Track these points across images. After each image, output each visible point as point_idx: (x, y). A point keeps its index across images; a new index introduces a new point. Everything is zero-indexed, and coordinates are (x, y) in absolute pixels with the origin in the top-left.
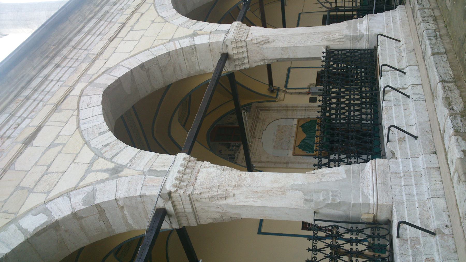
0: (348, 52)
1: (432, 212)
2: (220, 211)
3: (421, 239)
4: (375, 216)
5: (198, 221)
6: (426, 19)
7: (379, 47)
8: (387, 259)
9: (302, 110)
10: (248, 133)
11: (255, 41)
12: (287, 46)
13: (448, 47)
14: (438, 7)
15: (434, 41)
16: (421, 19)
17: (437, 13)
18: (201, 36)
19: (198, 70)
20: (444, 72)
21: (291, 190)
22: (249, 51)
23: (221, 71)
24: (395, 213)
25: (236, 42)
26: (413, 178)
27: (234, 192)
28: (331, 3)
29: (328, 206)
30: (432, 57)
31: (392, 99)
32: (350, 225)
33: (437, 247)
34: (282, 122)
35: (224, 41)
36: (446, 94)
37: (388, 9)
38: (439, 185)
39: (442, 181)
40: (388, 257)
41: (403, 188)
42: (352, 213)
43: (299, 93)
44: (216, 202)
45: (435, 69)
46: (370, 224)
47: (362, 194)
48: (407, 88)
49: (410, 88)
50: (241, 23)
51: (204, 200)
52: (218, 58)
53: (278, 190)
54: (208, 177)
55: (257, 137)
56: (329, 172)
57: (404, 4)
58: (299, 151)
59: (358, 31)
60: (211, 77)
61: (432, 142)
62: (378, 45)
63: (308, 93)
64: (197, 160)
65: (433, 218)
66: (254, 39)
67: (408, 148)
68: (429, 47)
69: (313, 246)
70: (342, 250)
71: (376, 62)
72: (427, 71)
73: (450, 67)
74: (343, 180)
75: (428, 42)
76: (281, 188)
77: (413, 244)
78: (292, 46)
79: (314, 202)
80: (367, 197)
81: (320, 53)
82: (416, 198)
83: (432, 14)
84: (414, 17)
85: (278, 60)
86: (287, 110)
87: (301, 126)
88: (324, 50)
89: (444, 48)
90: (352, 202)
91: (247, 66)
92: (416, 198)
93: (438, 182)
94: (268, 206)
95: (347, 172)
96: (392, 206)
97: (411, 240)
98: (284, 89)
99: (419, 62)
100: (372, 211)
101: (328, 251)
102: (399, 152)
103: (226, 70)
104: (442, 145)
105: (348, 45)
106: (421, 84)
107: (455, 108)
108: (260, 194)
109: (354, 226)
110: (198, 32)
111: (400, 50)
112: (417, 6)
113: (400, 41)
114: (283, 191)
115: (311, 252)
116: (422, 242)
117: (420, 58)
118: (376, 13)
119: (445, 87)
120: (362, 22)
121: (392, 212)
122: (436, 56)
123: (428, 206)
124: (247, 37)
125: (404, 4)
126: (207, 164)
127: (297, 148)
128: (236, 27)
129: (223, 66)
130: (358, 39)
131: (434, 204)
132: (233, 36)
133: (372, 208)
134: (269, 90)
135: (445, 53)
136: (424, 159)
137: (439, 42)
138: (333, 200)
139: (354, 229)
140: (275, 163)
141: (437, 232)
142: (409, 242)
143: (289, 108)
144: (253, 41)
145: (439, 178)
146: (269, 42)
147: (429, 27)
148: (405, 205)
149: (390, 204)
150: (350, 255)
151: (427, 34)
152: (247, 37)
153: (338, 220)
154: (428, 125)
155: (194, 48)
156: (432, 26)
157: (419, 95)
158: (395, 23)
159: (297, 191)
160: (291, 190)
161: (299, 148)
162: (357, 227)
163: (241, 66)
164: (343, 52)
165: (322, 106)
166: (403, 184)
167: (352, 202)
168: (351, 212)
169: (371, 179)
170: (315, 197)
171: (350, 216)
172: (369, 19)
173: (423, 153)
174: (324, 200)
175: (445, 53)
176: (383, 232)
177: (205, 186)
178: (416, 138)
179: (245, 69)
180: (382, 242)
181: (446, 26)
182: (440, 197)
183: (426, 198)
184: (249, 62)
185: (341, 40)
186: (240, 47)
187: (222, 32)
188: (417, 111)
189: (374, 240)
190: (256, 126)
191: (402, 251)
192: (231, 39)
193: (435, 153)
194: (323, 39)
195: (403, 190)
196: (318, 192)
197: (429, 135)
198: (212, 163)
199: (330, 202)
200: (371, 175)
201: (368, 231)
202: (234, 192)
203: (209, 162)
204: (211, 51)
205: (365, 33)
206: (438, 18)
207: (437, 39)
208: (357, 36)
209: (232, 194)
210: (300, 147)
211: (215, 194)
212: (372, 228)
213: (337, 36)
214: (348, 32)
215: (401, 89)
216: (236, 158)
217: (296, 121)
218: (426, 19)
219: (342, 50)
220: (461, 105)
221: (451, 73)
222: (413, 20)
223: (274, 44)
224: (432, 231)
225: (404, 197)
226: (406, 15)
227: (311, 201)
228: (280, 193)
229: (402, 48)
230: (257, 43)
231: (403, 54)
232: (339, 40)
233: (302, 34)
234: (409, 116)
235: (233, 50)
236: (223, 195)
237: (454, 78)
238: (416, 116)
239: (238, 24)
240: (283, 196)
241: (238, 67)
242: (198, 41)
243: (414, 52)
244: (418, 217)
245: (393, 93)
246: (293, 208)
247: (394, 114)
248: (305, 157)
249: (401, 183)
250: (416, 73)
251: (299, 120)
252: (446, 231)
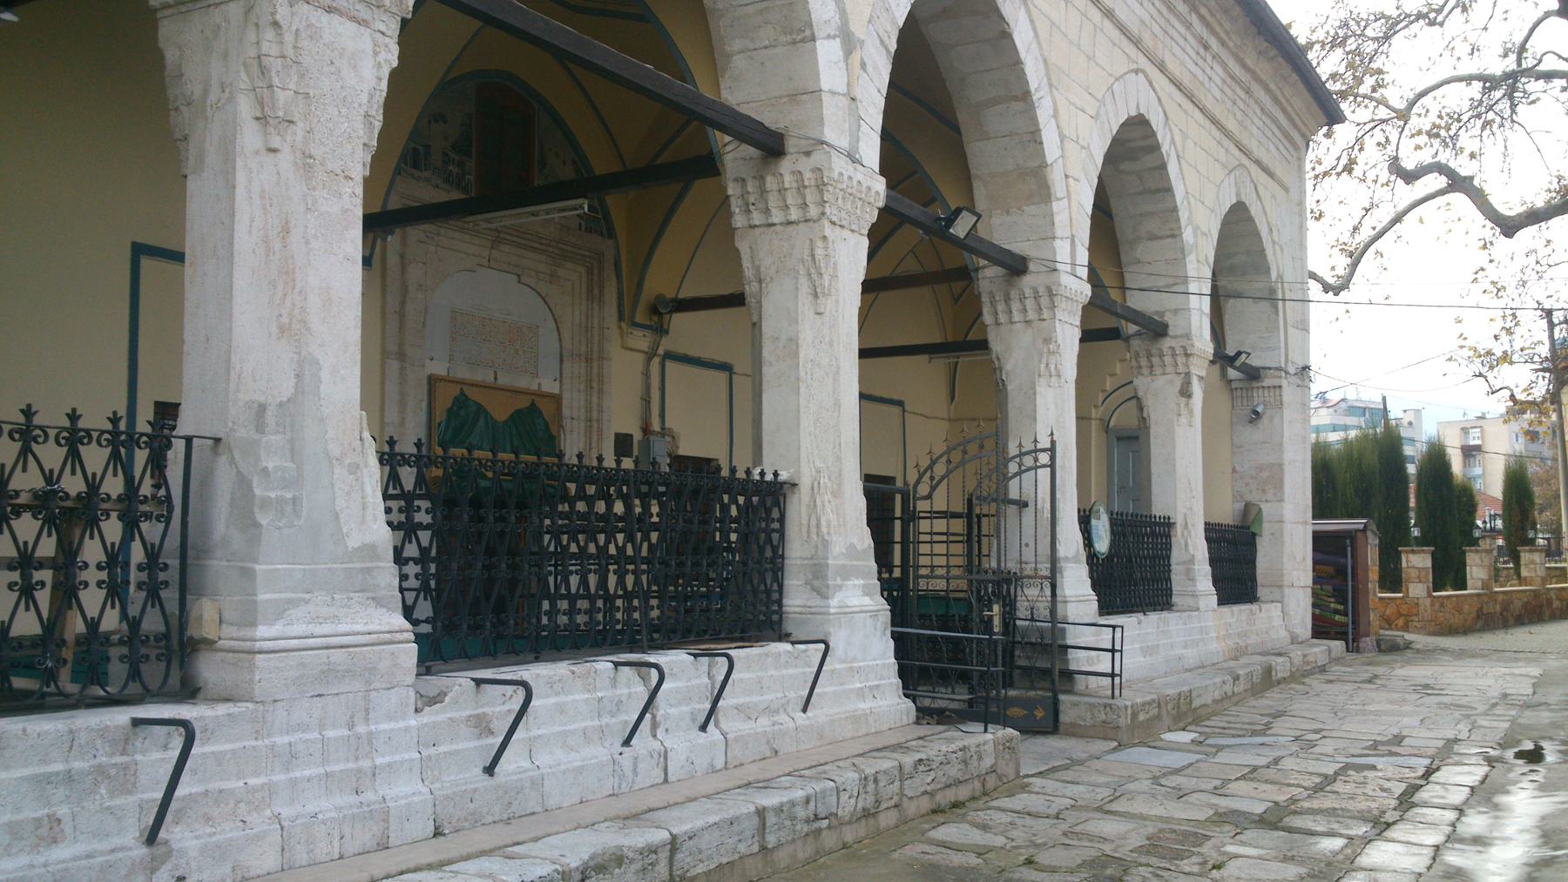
0: (775, 549)
1: (229, 831)
2: (212, 98)
3: (130, 799)
4: (209, 643)
5: (170, 11)
6: (871, 787)
7: (788, 647)
8: (52, 688)
9: (589, 409)
10: (506, 219)
11: (819, 252)
12: (802, 355)
13: (782, 857)
14: (904, 821)
15: (801, 813)
16: (869, 771)
17: (887, 819)
18: (842, 65)
19: (728, 49)
20: (704, 847)
21: (296, 357)
22: (790, 228)
23: (724, 129)
24: (222, 709)
25: (821, 186)
26: (351, 765)
27: (286, 149)
28: (929, 497)
29: (244, 483)
30: (753, 809)
31: (618, 692)
32: (174, 563)
33: (102, 853)
34: (548, 342)
35: (823, 143)
36: (631, 855)
37: (903, 673)
38: (325, 848)
39: (341, 858)
40: (60, 693)
42: (218, 565)
43: (646, 401)
44: (244, 82)
45: (716, 818)
46: (183, 627)
47: (289, 601)
48: (654, 736)
49: (656, 745)
50: (881, 204)
51: (251, 36)
52: (770, 119)
53: (297, 311)
54: (341, 55)
55: (495, 253)
56: (369, 490)
57: (918, 722)
59: (839, 581)
60: (706, 91)
61: (476, 821)
62: (793, 643)
63: (646, 430)
64: (404, 22)
65: (210, 835)
66: (826, 248)
67: (454, 747)
68: (785, 799)
69: (88, 432)
70: (78, 532)
71: (742, 639)
72: (708, 797)
73: (720, 866)
75: (799, 794)
76: (303, 322)
77: (113, 772)
78: (802, 373)
79: (257, 436)
80: (278, 616)
81: (774, 464)
82: (279, 777)
83: (884, 806)
84: (878, 750)
85: (756, 326)
86: (589, 360)
87: (533, 404)
88: (784, 476)
89: (780, 845)
90: (258, 567)
91: (739, 221)
92: (279, 777)
93: (336, 844)
94: (237, 274)
95: (369, 550)
96: (250, 700)
97: (125, 767)
98: (661, 351)
99: (738, 772)
100: (229, 635)
101: (73, 485)
102: (441, 717)
103: (729, 148)
104: (465, 851)
105: (796, 551)
106: (666, 781)
108: (278, 246)
109: (172, 575)
110: (856, 57)
111: (777, 711)
112: (908, 760)
113: (804, 710)
114: (292, 330)
115: (67, 423)
116: (118, 802)
117: (752, 772)
118: (894, 636)
119: (655, 852)
120: (867, 592)
121: (227, 700)
122: (756, 820)
123: (253, 818)
124: (833, 223)
125: (918, 722)
126: (391, 56)
127: (455, 391)
128: (869, 188)
129: (741, 138)
130: (816, 583)
131: (260, 837)
132: (841, 174)
133: (241, 634)
134: (660, 298)
135: (763, 848)
136: (416, 799)
137: (798, 827)
138: (266, 504)
139: (162, 576)
140: (401, 314)
141: (158, 850)
142: (119, 759)
143: (595, 364)
144: (820, 243)
145: (350, 849)
146: (816, 296)
147: (844, 797)
148: (254, 743)
149: (257, 692)
150: (61, 560)
151: (824, 791)
152: (833, 223)
153: (190, 519)
154: (533, 805)
155: (801, 35)
156: (847, 806)
158: (860, 694)
159: (293, 381)
160: (296, 357)
161: (456, 399)
162: (166, 583)
163: (740, 202)
164: (775, 536)
165: (599, 468)
166: (330, 733)
167: (258, 567)
168: (225, 563)
169: (342, 628)
170: (274, 439)
171: (209, 562)
172: (874, 614)
173: (437, 793)
174: (265, 470)
175: (763, 848)
176: (153, 672)
177: (304, 43)
178: (490, 770)
179: (730, 215)
180: (117, 670)
181: (845, 846)
182: (286, 855)
183: (277, 810)
184: (752, 227)
185: (814, 530)
186: (804, 197)
187: (855, 139)
188: (580, 770)
189: (121, 642)
190: (534, 249)
191: (83, 738)
192: (830, 169)
193: (438, 833)
194: (818, 471)
195: (307, 736)
196: (292, 450)
198: (394, 76)
199: (257, 491)
200: (359, 628)
201: (152, 623)
202: (286, 149)
203: (395, 64)
204: (793, 97)
205: (834, 602)
206: (872, 821)
207: (808, 821)
208: (825, 577)
209: (276, 142)
210: (461, 401)
211: (276, 81)
212: (166, 636)
213: (829, 516)
214: (838, 547)
215: (654, 717)
217: (550, 386)
218: (871, 787)
219: (782, 532)
221: (700, 869)
222: (867, 748)
223: (810, 314)
224: (162, 834)
225: (282, 740)
226: (886, 727)
227: (260, 428)
228: (285, 320)
229: (782, 718)
230: (813, 256)
231: (764, 723)
232: (813, 522)
233: (837, 404)
235: (793, 173)
236: (273, 108)
237: (682, 878)
238: (563, 767)
239: (877, 193)
240: (274, 330)
241: (739, 191)
242: (828, 52)
243: (768, 754)
244: (210, 786)
245: (641, 692)
246: (228, 361)
247: (570, 698)
248: (423, 417)
249: (334, 726)
250: (702, 764)
251: (556, 399)
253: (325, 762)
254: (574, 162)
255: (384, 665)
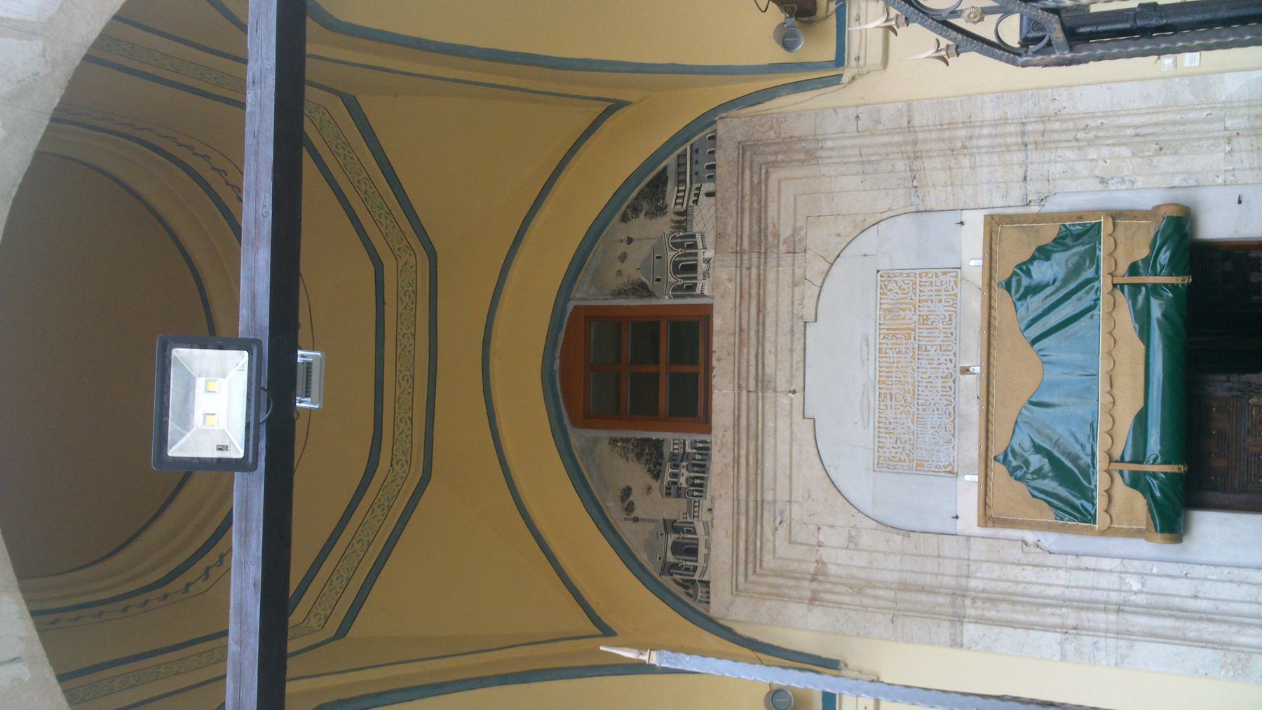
55: (782, 384)
58: (1009, 491)
190: (761, 308)
216: (702, 550)
254: (625, 219)
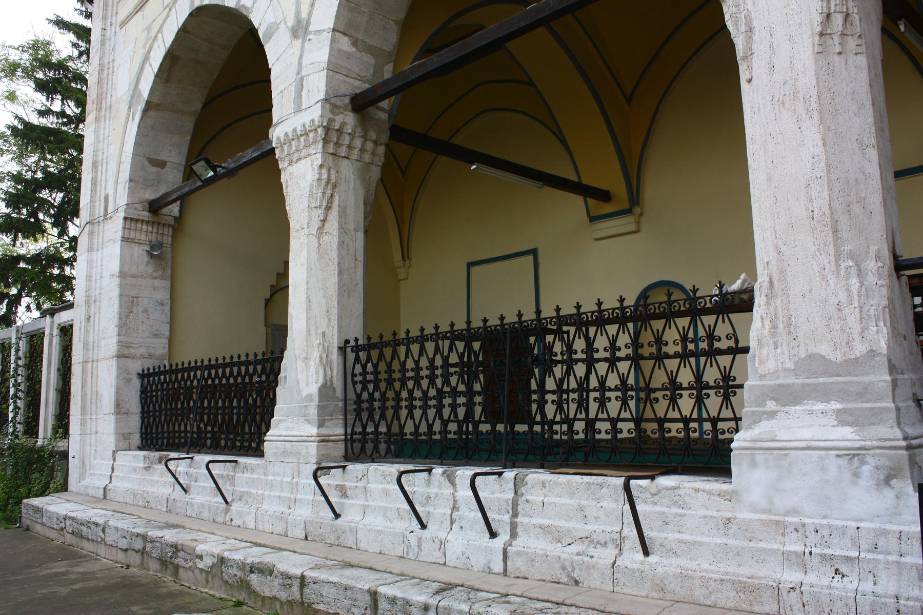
20: (324, 593)
41: (279, 478)
74: (299, 392)
107: (252, 575)
154: (350, 542)
157: (416, 549)
188: (380, 532)
197: (332, 540)
200: (297, 434)
220: (258, 589)
234: (384, 515)
237: (310, 605)
238: (369, 527)
250: (478, 561)
252: (228, 518)
253: (282, 491)
255: (304, 451)
